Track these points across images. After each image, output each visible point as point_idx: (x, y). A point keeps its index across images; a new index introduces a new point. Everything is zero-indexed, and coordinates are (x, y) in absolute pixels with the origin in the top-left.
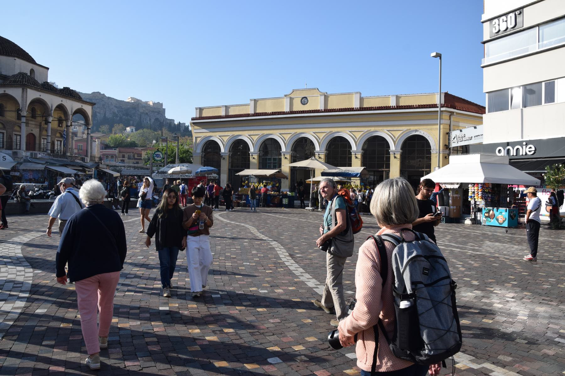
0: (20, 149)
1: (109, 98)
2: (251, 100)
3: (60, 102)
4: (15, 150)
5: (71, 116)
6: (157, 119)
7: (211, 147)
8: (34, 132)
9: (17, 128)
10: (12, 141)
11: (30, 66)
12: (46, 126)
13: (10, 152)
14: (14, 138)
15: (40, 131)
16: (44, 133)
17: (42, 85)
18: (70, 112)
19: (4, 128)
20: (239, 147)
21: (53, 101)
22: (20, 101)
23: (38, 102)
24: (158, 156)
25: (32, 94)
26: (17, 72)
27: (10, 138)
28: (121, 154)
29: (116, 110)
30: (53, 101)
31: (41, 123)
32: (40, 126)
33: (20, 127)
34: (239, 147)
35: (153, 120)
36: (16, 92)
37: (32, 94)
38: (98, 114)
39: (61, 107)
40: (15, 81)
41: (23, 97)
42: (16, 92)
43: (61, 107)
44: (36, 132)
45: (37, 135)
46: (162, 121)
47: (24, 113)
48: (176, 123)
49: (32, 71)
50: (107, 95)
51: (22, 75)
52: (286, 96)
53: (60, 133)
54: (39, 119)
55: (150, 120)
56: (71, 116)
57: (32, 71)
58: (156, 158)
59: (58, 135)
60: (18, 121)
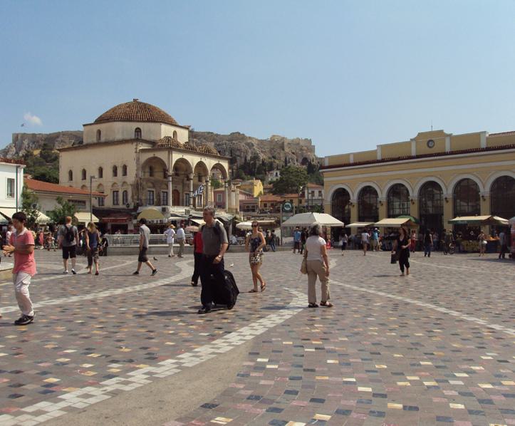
0: (167, 205)
2: (378, 146)
3: (199, 160)
4: (164, 207)
6: (305, 161)
7: (341, 195)
9: (164, 186)
10: (160, 199)
11: (173, 129)
12: (188, 182)
14: (162, 194)
16: (187, 188)
17: (184, 145)
19: (154, 187)
21: (193, 160)
22: (166, 163)
23: (182, 161)
25: (176, 156)
26: (162, 137)
27: (159, 195)
29: (258, 151)
30: (193, 160)
31: (183, 180)
33: (167, 186)
35: (300, 160)
36: (162, 155)
37: (176, 156)
39: (201, 165)
40: (162, 145)
42: (162, 155)
43: (201, 165)
44: (180, 188)
45: (181, 191)
47: (171, 172)
49: (175, 133)
50: (247, 135)
51: (168, 138)
52: (411, 140)
54: (182, 177)
56: (209, 172)
57: (175, 133)
60: (165, 180)
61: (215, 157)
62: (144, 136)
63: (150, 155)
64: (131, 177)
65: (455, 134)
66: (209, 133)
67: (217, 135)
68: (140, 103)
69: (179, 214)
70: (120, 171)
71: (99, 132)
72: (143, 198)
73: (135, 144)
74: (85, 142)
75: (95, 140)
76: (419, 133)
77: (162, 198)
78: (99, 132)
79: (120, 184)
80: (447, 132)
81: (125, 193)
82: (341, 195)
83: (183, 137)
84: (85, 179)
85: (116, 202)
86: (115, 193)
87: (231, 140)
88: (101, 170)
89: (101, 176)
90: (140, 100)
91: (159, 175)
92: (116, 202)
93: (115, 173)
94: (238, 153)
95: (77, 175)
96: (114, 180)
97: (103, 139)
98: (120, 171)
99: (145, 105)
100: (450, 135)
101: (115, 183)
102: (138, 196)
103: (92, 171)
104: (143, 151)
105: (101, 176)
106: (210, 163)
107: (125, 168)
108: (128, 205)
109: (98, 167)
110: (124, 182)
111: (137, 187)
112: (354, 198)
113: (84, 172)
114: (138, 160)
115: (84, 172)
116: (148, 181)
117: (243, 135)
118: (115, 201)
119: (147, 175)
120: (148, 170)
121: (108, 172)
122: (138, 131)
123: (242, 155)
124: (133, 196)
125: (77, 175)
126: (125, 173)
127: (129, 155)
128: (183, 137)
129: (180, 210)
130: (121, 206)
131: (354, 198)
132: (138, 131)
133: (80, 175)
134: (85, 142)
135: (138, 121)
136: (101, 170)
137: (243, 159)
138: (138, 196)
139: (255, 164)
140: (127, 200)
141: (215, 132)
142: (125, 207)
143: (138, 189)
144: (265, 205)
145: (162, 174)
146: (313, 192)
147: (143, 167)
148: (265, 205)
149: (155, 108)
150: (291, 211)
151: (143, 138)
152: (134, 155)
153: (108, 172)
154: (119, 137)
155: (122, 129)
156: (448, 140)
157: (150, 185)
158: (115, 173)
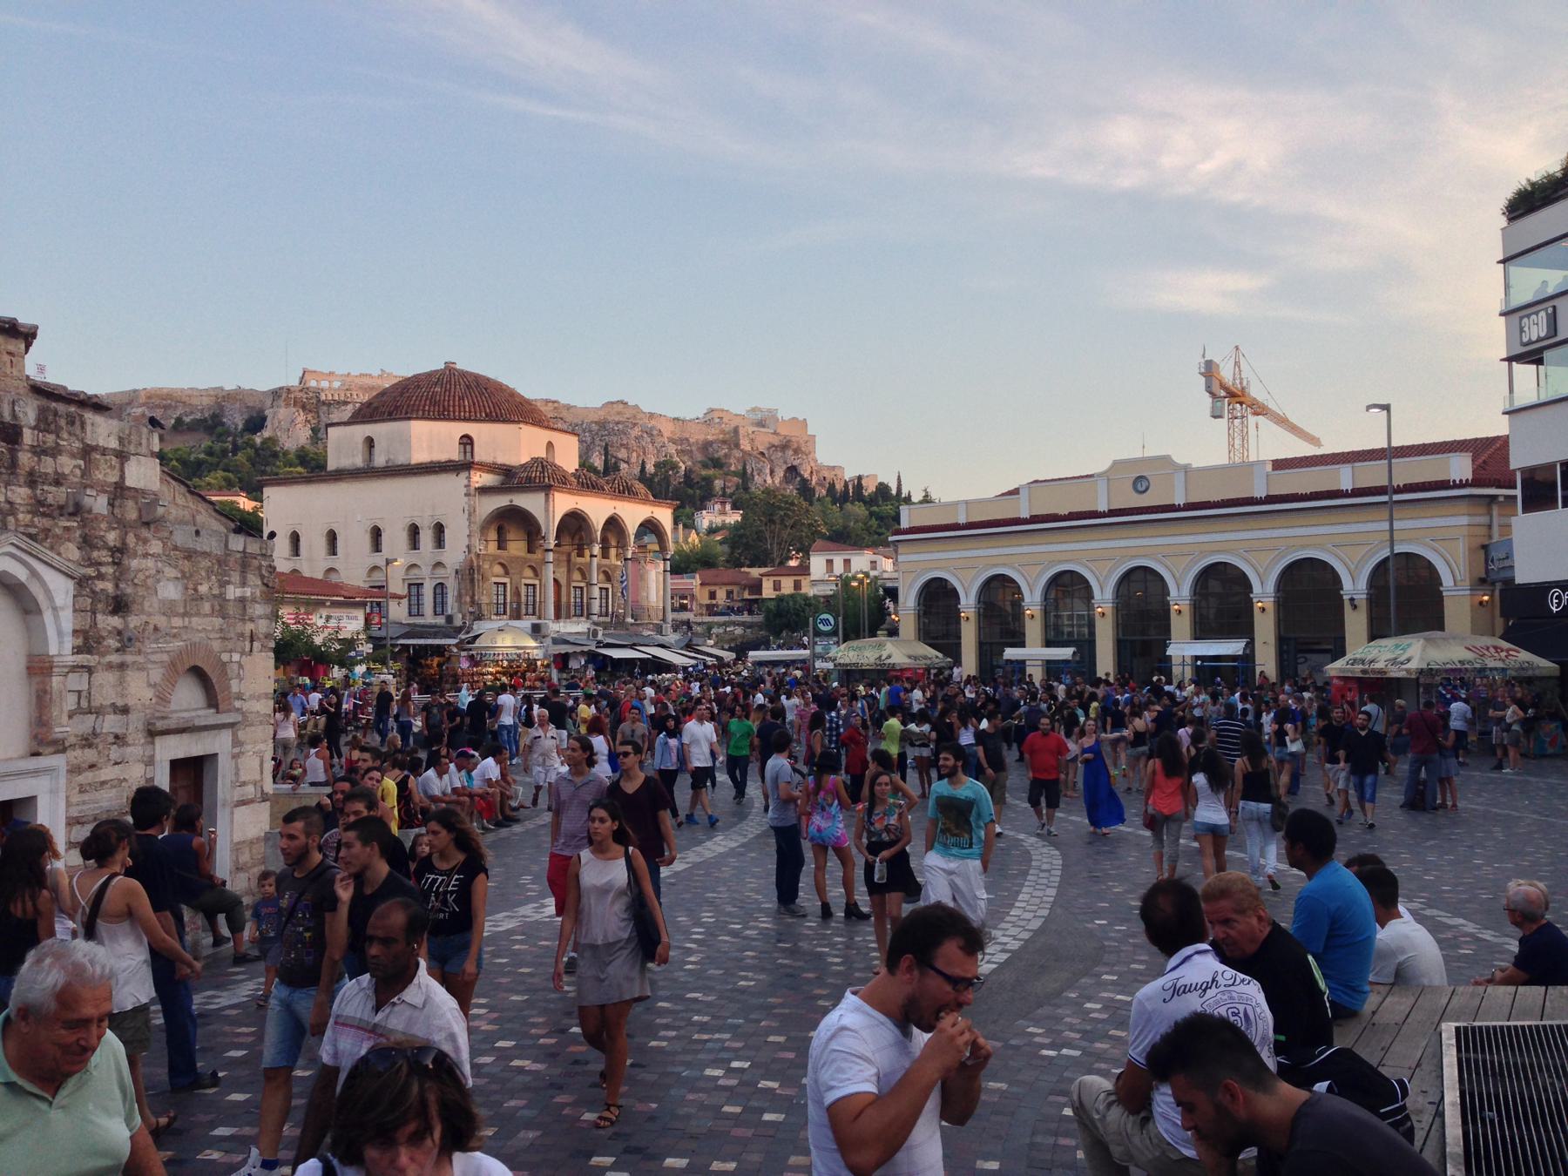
1: (651, 416)
5: (632, 538)
6: (792, 470)
7: (938, 596)
8: (558, 576)
9: (528, 572)
10: (519, 604)
11: (544, 435)
12: (580, 560)
13: (526, 623)
14: (523, 590)
15: (569, 571)
18: (632, 526)
19: (507, 573)
20: (999, 593)
21: (598, 509)
24: (826, 622)
25: (563, 503)
27: (517, 593)
28: (706, 590)
29: (672, 449)
30: (598, 509)
32: (569, 561)
34: (999, 593)
35: (780, 473)
36: (530, 502)
37: (563, 503)
38: (623, 466)
39: (613, 524)
41: (547, 510)
42: (530, 502)
43: (613, 524)
45: (563, 582)
46: (806, 475)
48: (849, 474)
49: (550, 445)
50: (646, 408)
51: (537, 462)
53: (605, 573)
55: (772, 472)
57: (550, 445)
58: (821, 626)
59: (602, 577)
61: (645, 501)
62: (480, 455)
63: (502, 501)
64: (454, 554)
65: (1198, 462)
66: (547, 401)
67: (568, 407)
68: (464, 374)
69: (571, 639)
70: (426, 538)
71: (370, 442)
72: (485, 600)
73: (464, 475)
74: (332, 465)
75: (359, 461)
76: (1115, 463)
77: (523, 599)
78: (370, 442)
79: (425, 571)
80: (1180, 459)
81: (440, 588)
82: (938, 596)
83: (568, 456)
84: (334, 553)
85: (415, 611)
86: (414, 590)
87: (602, 424)
88: (376, 534)
89: (377, 545)
90: (463, 365)
91: (517, 547)
92: (415, 611)
93: (414, 543)
94: (622, 454)
95: (314, 544)
96: (413, 557)
97: (380, 460)
98: (426, 538)
99: (477, 377)
100: (1186, 469)
101: (414, 566)
102: (472, 597)
103: (354, 542)
104: (484, 490)
105: (377, 545)
106: (633, 514)
107: (439, 529)
108: (450, 619)
109: (369, 525)
110: (439, 564)
111: (470, 574)
112: (968, 603)
113: (332, 537)
115: (332, 537)
117: (636, 406)
118: (415, 609)
119: (493, 547)
120: (493, 535)
121: (395, 539)
122: (467, 441)
123: (634, 460)
124: (460, 597)
125: (314, 544)
126: (439, 542)
127: (453, 503)
128: (568, 456)
129: (575, 627)
130: (429, 618)
131: (968, 603)
132: (467, 441)
133: (321, 543)
134: (332, 465)
135: (466, 420)
136: (376, 534)
137: (637, 471)
138: (472, 597)
139: (667, 479)
140: (443, 603)
141: (563, 401)
142: (441, 620)
143: (472, 580)
144: (713, 595)
145: (523, 545)
146: (830, 562)
147: (484, 528)
148: (713, 595)
149: (500, 388)
150: (834, 633)
151: (477, 459)
153: (395, 539)
154: (419, 456)
155: (430, 439)
156: (1179, 478)
157: (498, 569)
158: (414, 543)
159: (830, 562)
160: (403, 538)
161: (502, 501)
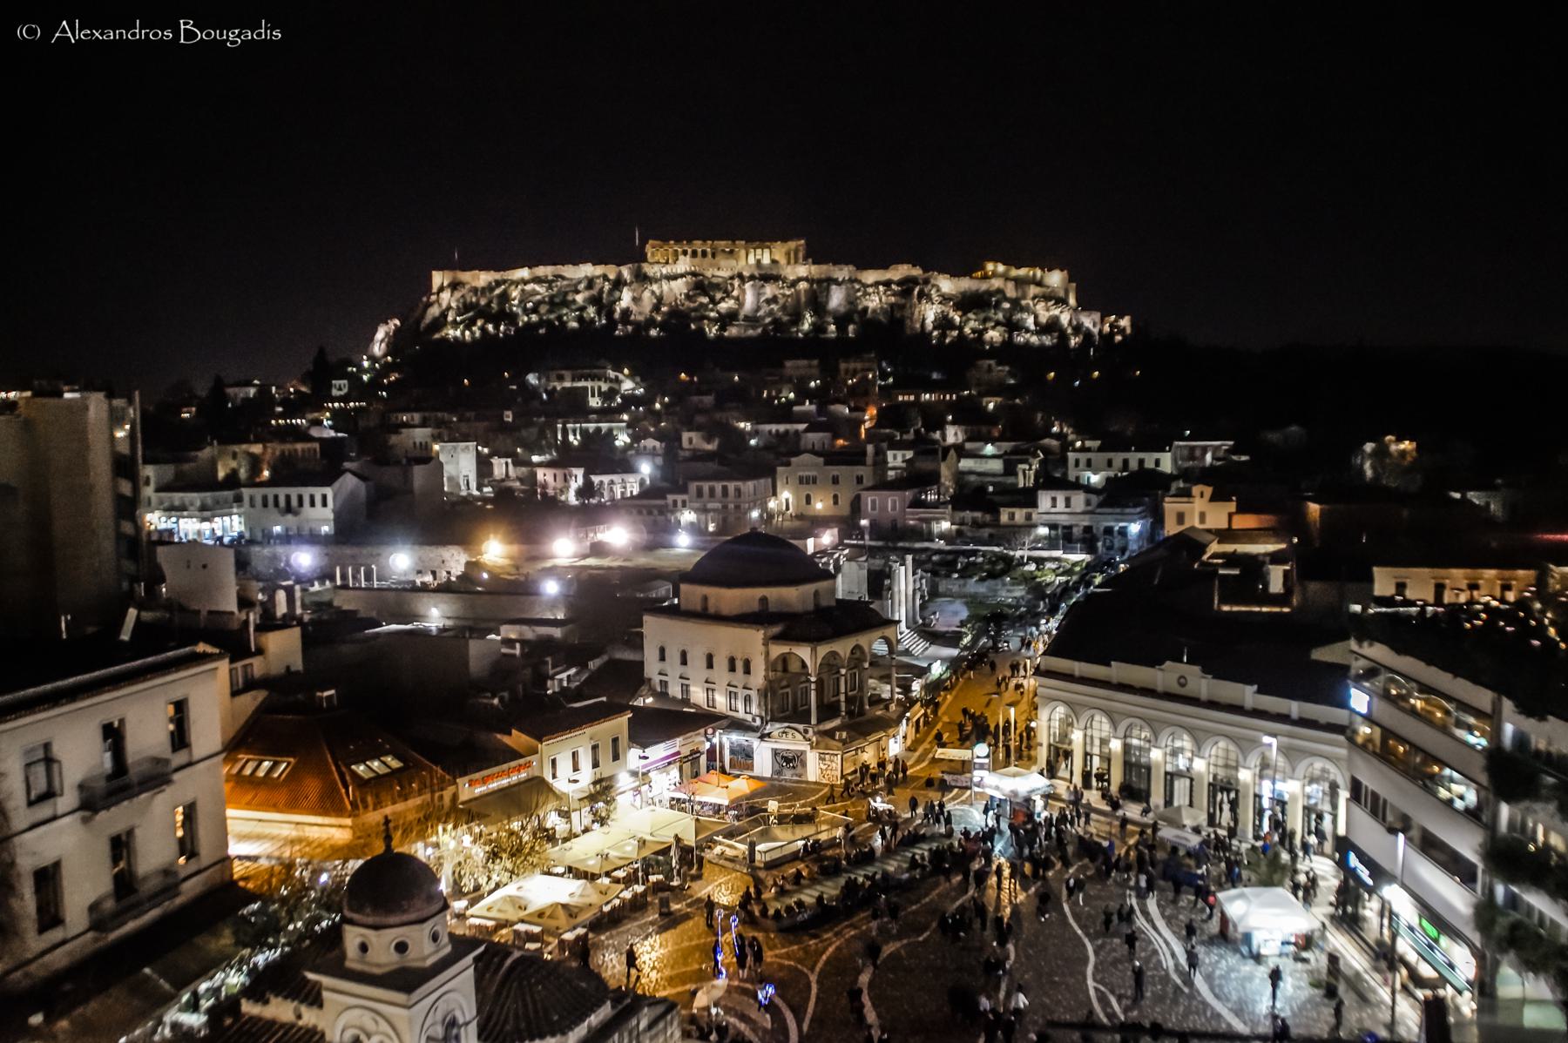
22: (808, 663)
37: (823, 650)
64: (758, 678)
70: (739, 665)
95: (673, 655)
97: (712, 610)
98: (739, 665)
114: (767, 654)
116: (781, 680)
120: (780, 667)
121: (721, 662)
125: (673, 655)
126: (747, 671)
146: (1054, 500)
152: (762, 648)
153: (721, 662)
158: (732, 669)
159: (1054, 500)
160: (725, 664)
161: (784, 649)
